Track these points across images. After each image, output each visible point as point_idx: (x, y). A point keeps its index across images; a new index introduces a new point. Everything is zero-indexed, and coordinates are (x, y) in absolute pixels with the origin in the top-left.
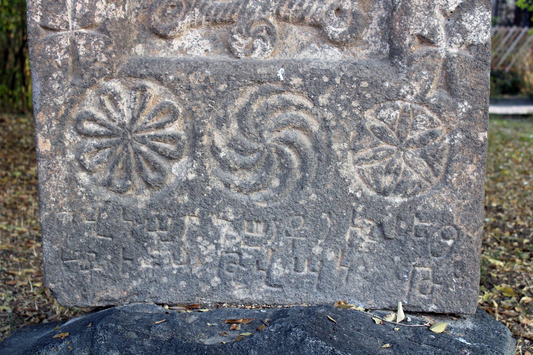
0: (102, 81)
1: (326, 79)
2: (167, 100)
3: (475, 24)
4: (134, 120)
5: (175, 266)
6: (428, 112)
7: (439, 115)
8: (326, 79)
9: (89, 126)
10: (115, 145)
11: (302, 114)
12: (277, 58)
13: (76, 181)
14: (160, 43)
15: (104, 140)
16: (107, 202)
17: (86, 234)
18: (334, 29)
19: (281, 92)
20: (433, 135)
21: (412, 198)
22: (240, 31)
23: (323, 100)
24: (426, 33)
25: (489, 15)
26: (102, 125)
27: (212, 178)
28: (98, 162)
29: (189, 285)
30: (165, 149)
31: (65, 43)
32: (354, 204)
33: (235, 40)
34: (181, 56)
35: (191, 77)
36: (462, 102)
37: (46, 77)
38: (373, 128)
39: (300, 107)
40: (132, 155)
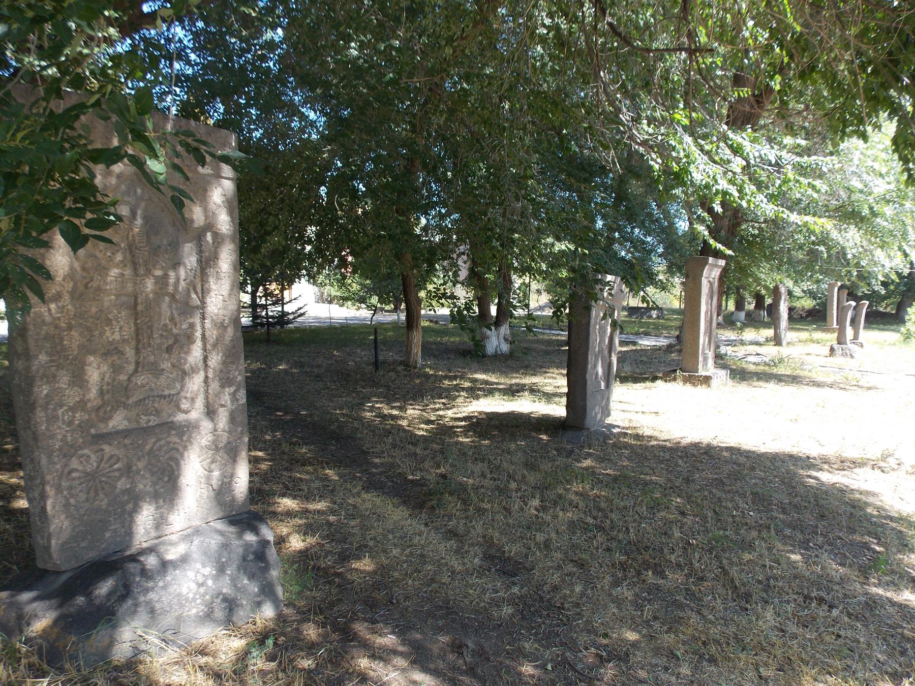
4: (98, 467)
10: (89, 481)
14: (102, 426)
28: (81, 492)
31: (59, 437)
37: (50, 456)
39: (175, 443)
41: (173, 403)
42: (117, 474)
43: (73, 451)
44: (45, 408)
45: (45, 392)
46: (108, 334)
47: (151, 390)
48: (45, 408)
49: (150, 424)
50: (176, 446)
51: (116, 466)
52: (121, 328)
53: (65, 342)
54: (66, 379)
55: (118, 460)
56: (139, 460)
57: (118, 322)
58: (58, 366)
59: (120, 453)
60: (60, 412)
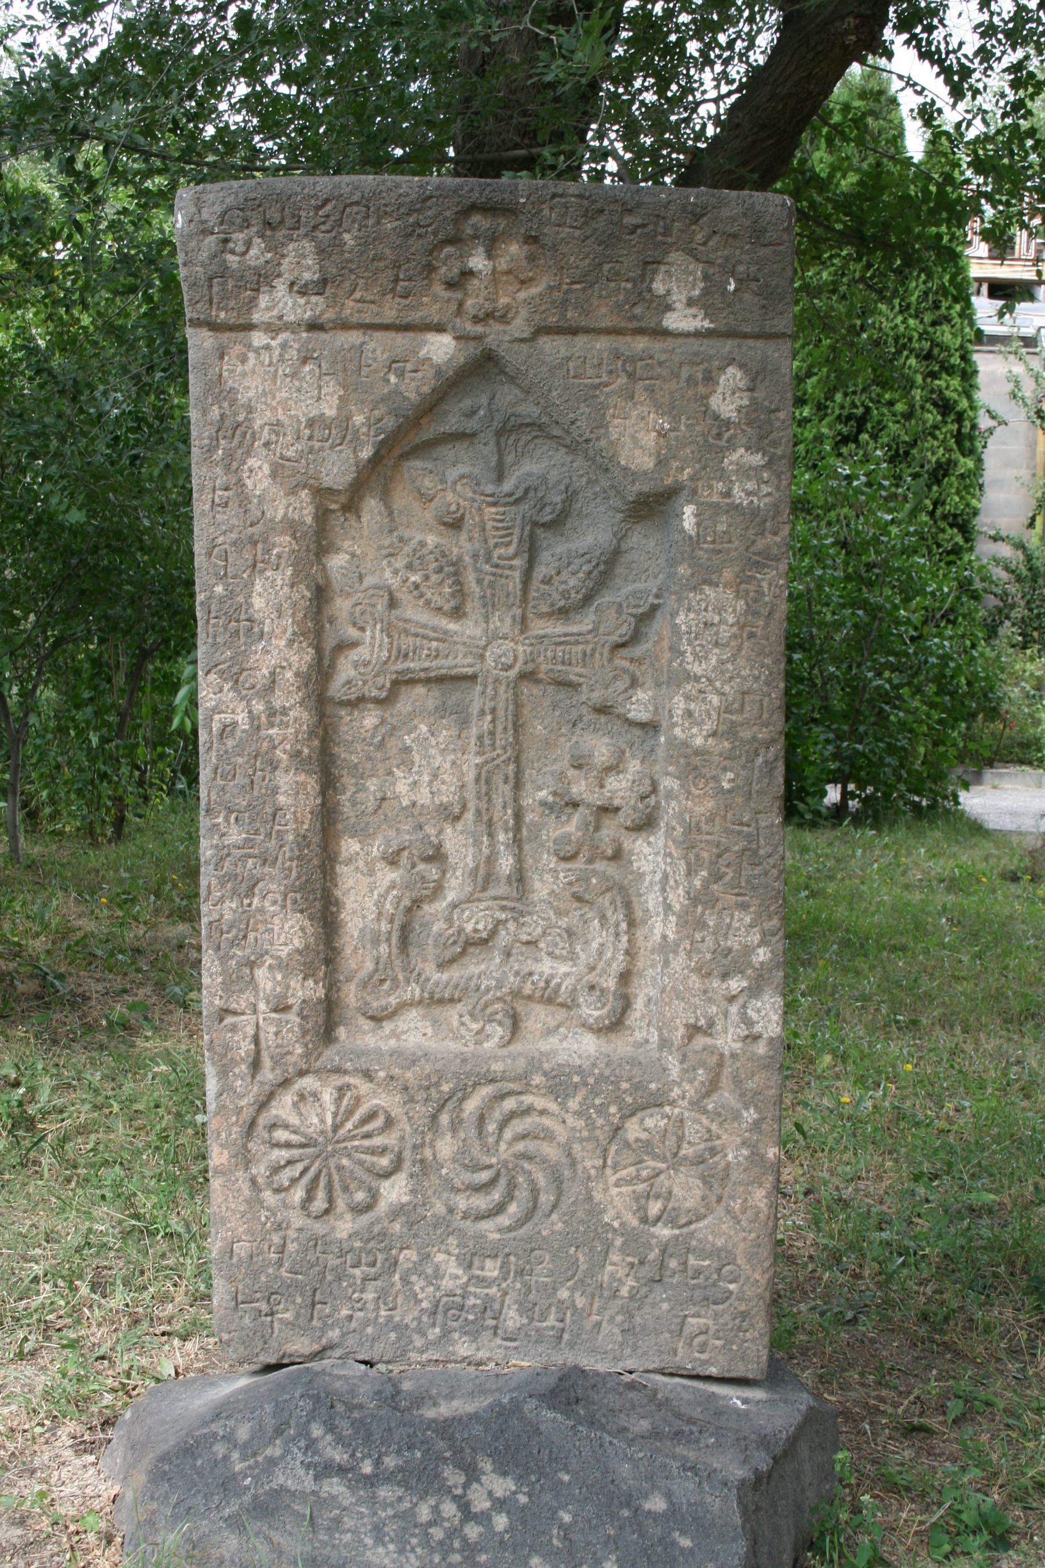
2: (375, 1101)
4: (336, 1128)
8: (576, 1079)
9: (281, 1135)
11: (546, 1121)
15: (296, 1152)
16: (300, 1230)
19: (520, 1093)
20: (713, 1151)
21: (685, 1230)
23: (573, 1104)
24: (702, 1022)
25: (779, 1001)
26: (295, 1132)
29: (399, 1339)
30: (373, 1164)
31: (250, 1031)
33: (463, 1024)
38: (637, 1140)
39: (543, 1112)
40: (334, 1172)
42: (385, 1162)
45: (228, 916)
46: (402, 787)
50: (546, 1121)
52: (435, 776)
53: (282, 799)
55: (389, 1123)
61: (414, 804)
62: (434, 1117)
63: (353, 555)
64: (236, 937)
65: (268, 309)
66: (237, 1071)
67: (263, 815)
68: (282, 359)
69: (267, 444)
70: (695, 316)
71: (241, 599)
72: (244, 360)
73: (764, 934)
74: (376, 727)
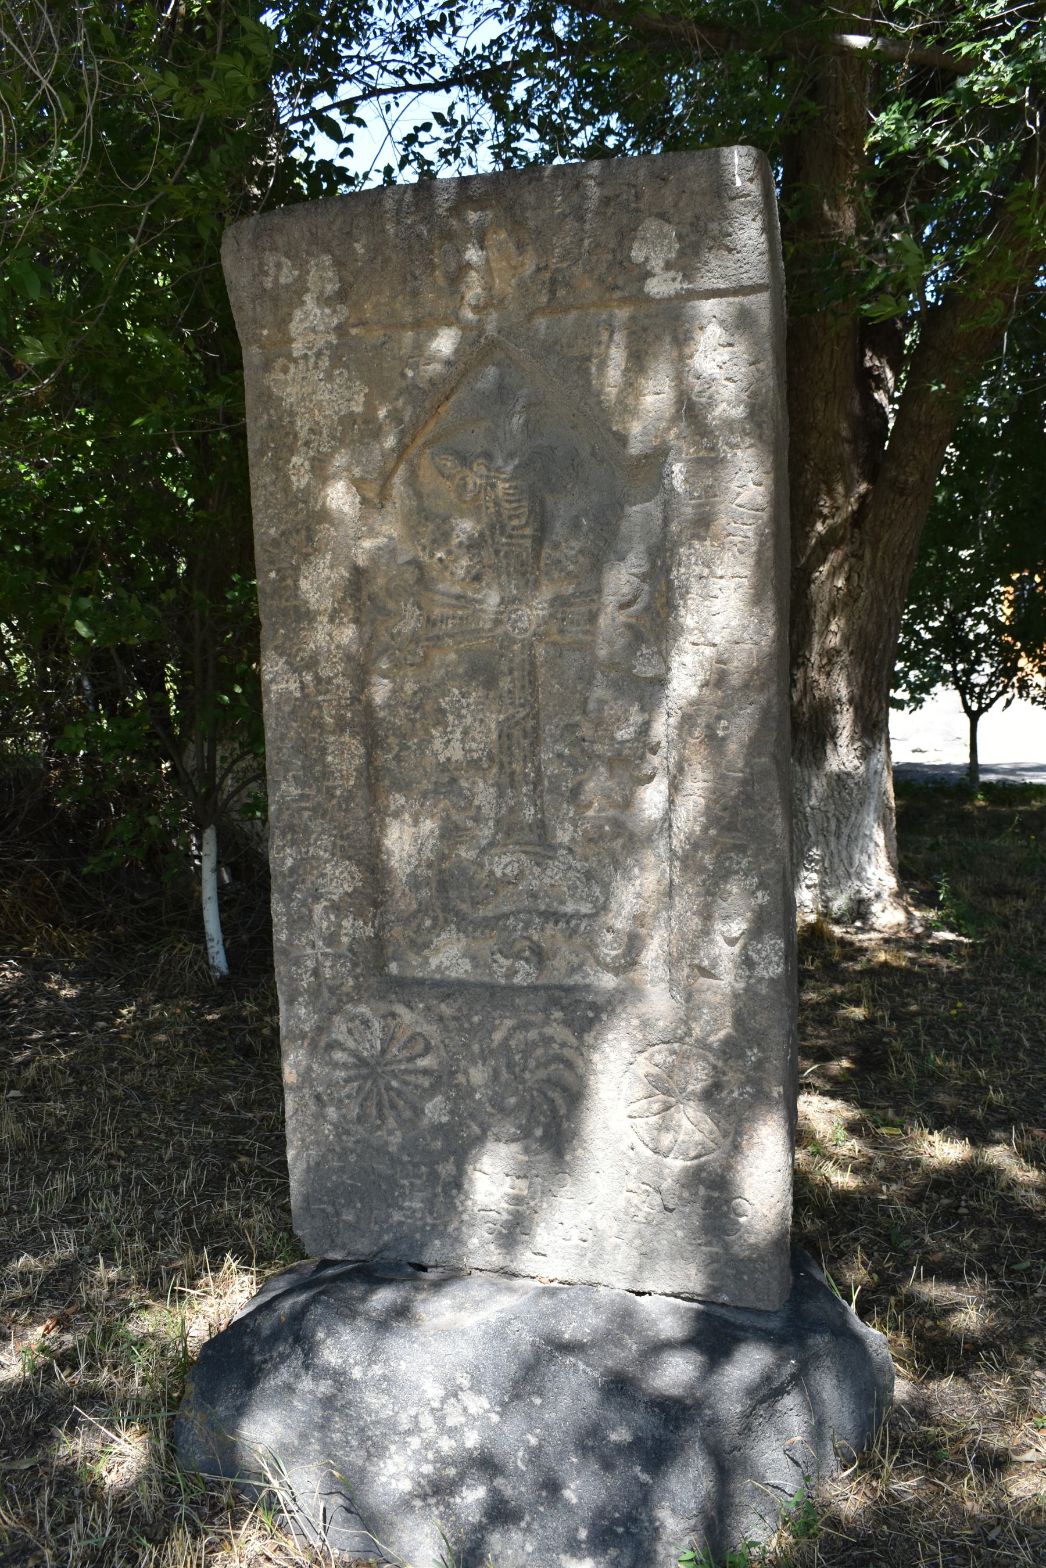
0: (349, 1007)
1: (591, 1014)
2: (418, 1030)
3: (764, 954)
4: (383, 1051)
5: (429, 1220)
6: (712, 1059)
7: (726, 1061)
10: (365, 1078)
12: (543, 981)
13: (324, 1117)
17: (334, 1178)
18: (606, 951)
22: (501, 952)
24: (706, 963)
27: (469, 1122)
31: (310, 964)
32: (626, 1164)
33: (495, 961)
34: (438, 976)
35: (443, 1006)
36: (751, 1048)
39: (563, 1045)
41: (578, 940)
43: (334, 1001)
44: (288, 898)
45: (289, 862)
46: (438, 744)
47: (533, 895)
48: (288, 898)
49: (517, 980)
51: (423, 1063)
52: (465, 733)
53: (330, 758)
54: (326, 840)
55: (427, 1049)
56: (474, 1063)
57: (460, 717)
58: (314, 810)
59: (430, 1029)
60: (318, 908)
61: (449, 759)
62: (466, 1046)
63: (391, 538)
64: (296, 882)
65: (301, 321)
66: (301, 999)
67: (315, 772)
68: (316, 366)
69: (307, 444)
70: (674, 280)
71: (289, 582)
72: (285, 370)
73: (761, 876)
74: (415, 693)
